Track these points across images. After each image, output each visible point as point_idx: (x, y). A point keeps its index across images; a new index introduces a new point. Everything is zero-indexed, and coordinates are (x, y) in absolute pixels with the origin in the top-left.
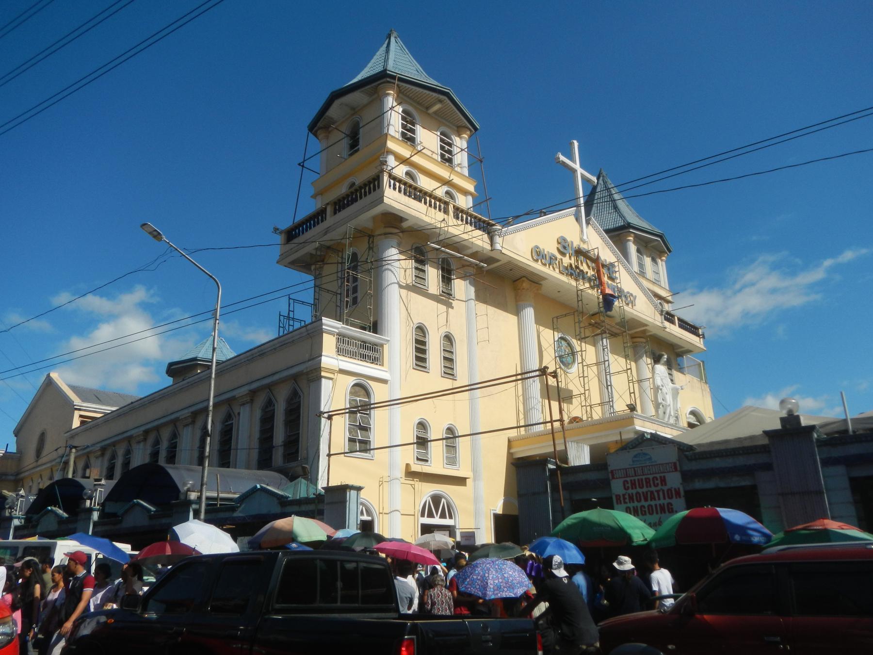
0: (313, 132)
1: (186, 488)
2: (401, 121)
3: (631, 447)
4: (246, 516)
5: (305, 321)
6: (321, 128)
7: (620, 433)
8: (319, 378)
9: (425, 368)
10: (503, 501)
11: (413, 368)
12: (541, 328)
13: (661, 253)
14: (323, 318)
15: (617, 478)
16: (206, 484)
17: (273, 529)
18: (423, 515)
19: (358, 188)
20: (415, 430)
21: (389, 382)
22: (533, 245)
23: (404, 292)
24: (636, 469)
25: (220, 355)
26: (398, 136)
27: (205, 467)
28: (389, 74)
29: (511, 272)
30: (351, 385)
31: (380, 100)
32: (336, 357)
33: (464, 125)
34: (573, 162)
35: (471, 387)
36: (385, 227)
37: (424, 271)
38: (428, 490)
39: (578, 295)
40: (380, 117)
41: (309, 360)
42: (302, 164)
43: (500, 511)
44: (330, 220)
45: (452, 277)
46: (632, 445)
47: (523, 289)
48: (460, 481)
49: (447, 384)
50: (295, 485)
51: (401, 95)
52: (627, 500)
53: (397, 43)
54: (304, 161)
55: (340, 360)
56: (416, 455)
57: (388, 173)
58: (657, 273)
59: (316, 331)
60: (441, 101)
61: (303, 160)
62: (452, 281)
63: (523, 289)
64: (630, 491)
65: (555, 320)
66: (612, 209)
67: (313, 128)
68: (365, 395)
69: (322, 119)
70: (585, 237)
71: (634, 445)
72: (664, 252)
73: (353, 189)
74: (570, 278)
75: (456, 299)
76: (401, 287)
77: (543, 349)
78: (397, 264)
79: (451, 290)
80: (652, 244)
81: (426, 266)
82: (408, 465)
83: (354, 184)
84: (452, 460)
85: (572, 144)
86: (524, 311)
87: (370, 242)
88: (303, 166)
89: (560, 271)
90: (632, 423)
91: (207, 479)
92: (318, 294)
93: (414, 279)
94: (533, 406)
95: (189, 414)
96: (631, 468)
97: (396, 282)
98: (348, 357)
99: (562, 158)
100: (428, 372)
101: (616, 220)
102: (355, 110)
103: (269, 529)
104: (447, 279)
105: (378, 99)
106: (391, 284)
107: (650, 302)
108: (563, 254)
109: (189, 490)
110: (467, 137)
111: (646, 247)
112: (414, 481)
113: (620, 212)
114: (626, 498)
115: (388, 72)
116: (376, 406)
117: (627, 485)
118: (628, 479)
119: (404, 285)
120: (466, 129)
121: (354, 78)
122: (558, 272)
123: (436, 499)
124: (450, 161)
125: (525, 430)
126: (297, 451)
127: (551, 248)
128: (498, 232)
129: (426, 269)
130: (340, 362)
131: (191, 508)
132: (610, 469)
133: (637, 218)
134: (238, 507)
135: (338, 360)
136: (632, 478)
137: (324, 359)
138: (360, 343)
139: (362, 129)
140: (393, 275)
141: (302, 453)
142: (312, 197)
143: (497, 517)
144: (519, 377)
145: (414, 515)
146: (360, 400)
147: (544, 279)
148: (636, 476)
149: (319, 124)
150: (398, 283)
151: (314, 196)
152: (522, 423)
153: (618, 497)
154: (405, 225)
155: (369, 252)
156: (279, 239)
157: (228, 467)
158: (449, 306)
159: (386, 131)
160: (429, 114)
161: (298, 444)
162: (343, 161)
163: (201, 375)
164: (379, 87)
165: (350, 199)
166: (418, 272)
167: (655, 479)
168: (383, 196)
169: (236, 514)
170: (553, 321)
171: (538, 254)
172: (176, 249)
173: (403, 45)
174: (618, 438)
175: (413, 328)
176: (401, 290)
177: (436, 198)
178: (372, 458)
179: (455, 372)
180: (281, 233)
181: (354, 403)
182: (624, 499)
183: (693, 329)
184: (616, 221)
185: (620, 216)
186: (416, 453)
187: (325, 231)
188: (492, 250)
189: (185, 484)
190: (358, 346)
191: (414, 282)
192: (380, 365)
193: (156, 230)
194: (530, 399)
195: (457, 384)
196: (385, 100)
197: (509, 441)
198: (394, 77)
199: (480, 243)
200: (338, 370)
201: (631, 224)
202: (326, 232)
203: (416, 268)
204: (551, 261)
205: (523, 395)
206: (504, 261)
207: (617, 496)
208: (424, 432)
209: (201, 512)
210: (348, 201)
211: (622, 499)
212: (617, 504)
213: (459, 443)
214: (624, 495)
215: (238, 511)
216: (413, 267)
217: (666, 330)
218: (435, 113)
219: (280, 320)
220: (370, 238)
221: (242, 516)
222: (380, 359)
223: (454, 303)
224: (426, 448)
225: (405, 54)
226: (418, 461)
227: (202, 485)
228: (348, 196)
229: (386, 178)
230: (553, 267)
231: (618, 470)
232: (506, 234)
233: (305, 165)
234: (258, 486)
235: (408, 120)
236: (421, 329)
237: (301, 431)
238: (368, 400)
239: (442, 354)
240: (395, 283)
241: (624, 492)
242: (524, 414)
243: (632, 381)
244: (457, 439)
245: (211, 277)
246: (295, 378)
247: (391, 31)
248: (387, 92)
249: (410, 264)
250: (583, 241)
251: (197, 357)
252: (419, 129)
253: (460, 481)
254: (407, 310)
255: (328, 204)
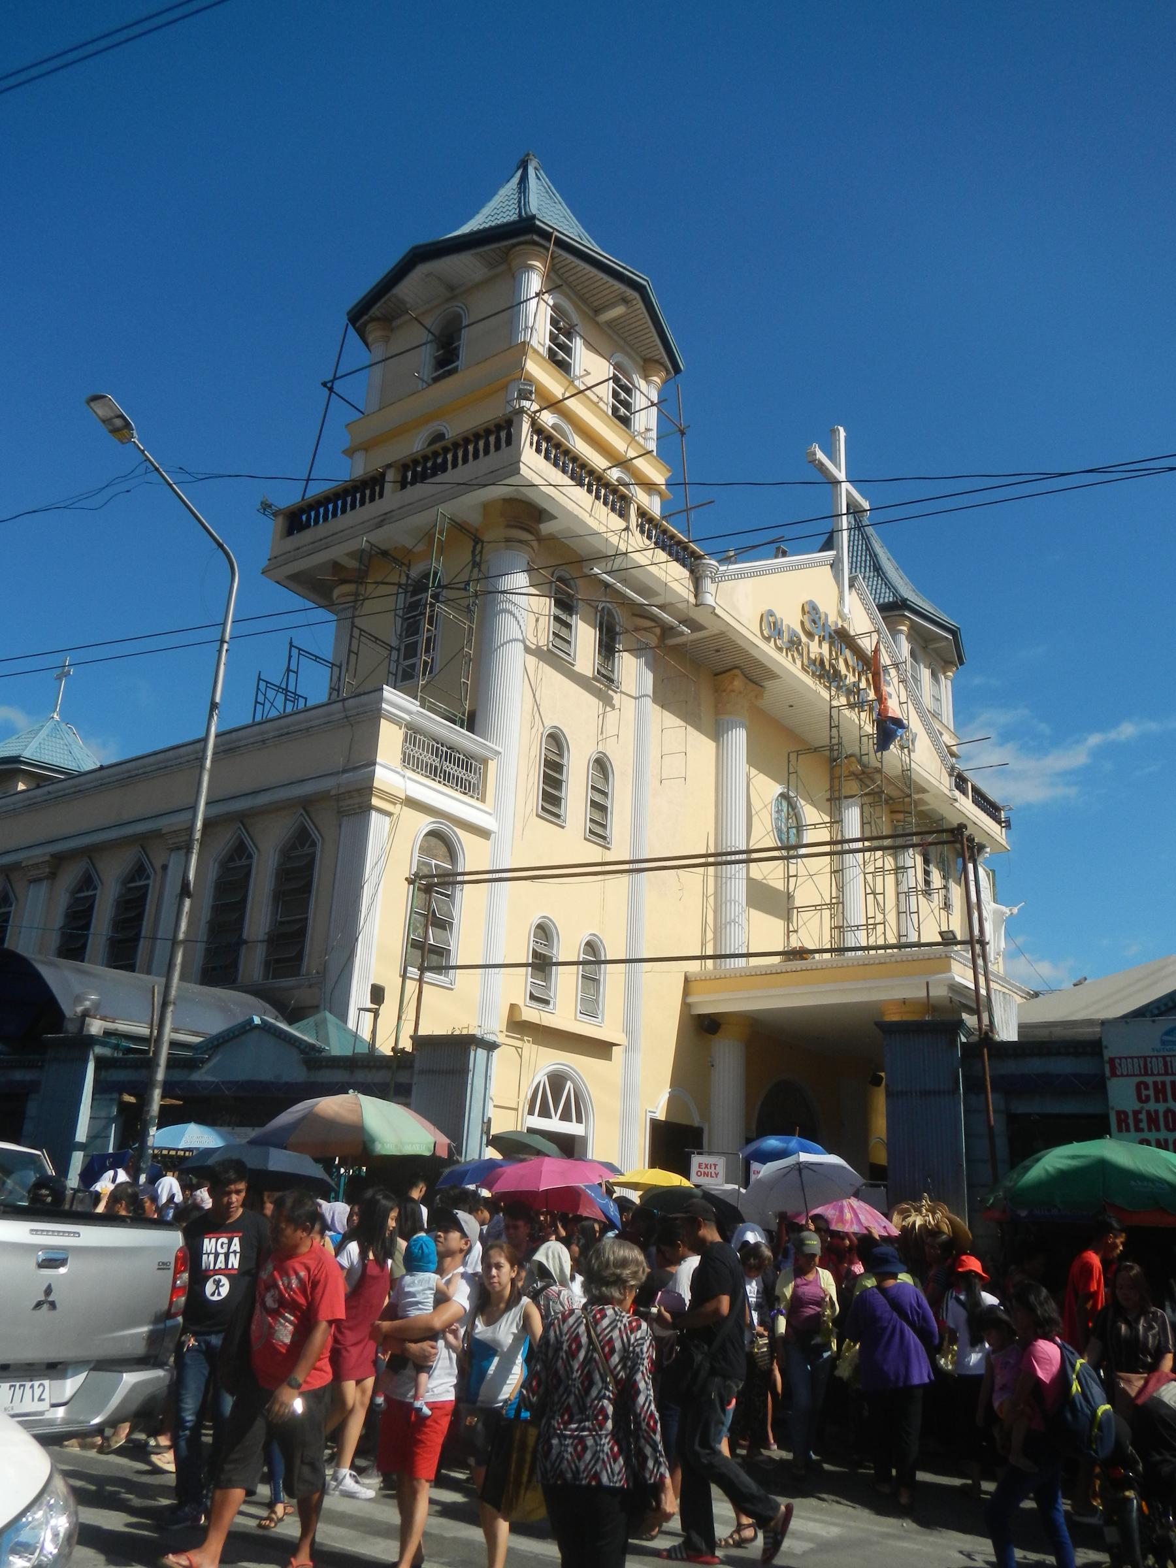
0: (358, 325)
1: (79, 1009)
2: (549, 327)
3: (1156, 1012)
4: (223, 1083)
5: (306, 699)
6: (376, 319)
7: (927, 984)
8: (366, 809)
9: (558, 816)
10: (668, 1095)
11: (538, 816)
12: (753, 772)
13: (947, 664)
14: (385, 686)
15: (1122, 1075)
16: (174, 1003)
17: (311, 1118)
18: (531, 1112)
19: (450, 446)
20: (532, 938)
21: (493, 835)
22: (765, 608)
23: (532, 660)
24: (1168, 1059)
25: (66, 757)
26: (543, 351)
27: (175, 965)
28: (538, 226)
29: (719, 654)
30: (424, 832)
31: (513, 276)
32: (402, 773)
33: (657, 357)
34: (836, 467)
35: (636, 867)
36: (509, 526)
37: (568, 626)
38: (549, 1060)
39: (831, 717)
40: (513, 306)
41: (344, 771)
42: (329, 385)
43: (661, 1116)
44: (392, 498)
45: (617, 646)
46: (1158, 1008)
47: (733, 691)
48: (601, 1049)
49: (593, 853)
50: (316, 1025)
51: (552, 275)
52: (1144, 1125)
53: (540, 179)
54: (335, 378)
55: (409, 779)
56: (529, 988)
57: (530, 416)
58: (938, 700)
59: (366, 712)
60: (625, 301)
61: (331, 378)
62: (617, 654)
63: (733, 691)
64: (1152, 1106)
65: (793, 757)
66: (870, 571)
67: (359, 316)
68: (445, 857)
69: (383, 300)
70: (846, 611)
71: (1163, 1008)
72: (952, 663)
73: (437, 446)
74: (818, 683)
75: (621, 692)
76: (527, 650)
77: (754, 812)
78: (521, 600)
79: (612, 671)
80: (937, 645)
81: (574, 616)
82: (513, 1007)
83: (440, 437)
84: (590, 1007)
85: (834, 432)
86: (730, 732)
87: (477, 552)
88: (331, 389)
89: (803, 665)
90: (949, 969)
91: (176, 991)
92: (357, 641)
93: (551, 639)
94: (733, 917)
95: (47, 858)
96: (1157, 1057)
97: (521, 638)
98: (422, 775)
99: (820, 455)
100: (563, 827)
101: (878, 591)
102: (453, 291)
103: (303, 1119)
104: (607, 649)
105: (513, 277)
106: (511, 641)
107: (935, 749)
108: (810, 635)
109: (86, 1014)
110: (659, 381)
111: (925, 648)
112: (523, 1040)
113: (887, 578)
114: (1141, 1121)
115: (538, 223)
116: (467, 878)
117: (1144, 1093)
118: (1149, 1080)
119: (533, 647)
120: (662, 368)
121: (464, 223)
122: (800, 668)
123: (557, 1081)
124: (625, 421)
125: (715, 964)
126: (299, 957)
127: (792, 620)
128: (711, 572)
129: (573, 624)
130: (410, 784)
131: (91, 1053)
132: (1107, 1054)
133: (914, 594)
134: (203, 1062)
135: (404, 777)
136: (1159, 1079)
137: (378, 769)
138: (445, 749)
139: (467, 329)
140: (516, 623)
141: (311, 963)
142: (344, 452)
143: (656, 1125)
144: (711, 860)
145: (516, 1110)
146: (436, 865)
147: (772, 676)
148: (1166, 1074)
149: (375, 311)
150: (523, 642)
151: (350, 452)
152: (710, 952)
153: (1122, 1116)
154: (546, 528)
155: (471, 572)
156: (271, 528)
157: (133, 971)
158: (608, 702)
159: (521, 339)
160: (597, 323)
161: (302, 943)
162: (420, 388)
163: (65, 783)
164: (514, 250)
165: (429, 464)
166: (558, 625)
167: (1142, 1086)
168: (519, 461)
169: (196, 1076)
170: (789, 757)
171: (772, 626)
172: (157, 469)
173: (550, 184)
174: (922, 994)
175: (542, 734)
176: (527, 655)
177: (607, 485)
178: (450, 986)
179: (608, 832)
180: (275, 514)
181: (425, 871)
182: (1137, 1121)
183: (990, 808)
184: (880, 594)
185: (886, 584)
186: (529, 984)
187: (382, 518)
188: (697, 605)
189: (79, 999)
190: (441, 756)
191: (550, 644)
192: (478, 799)
193: (122, 416)
194: (728, 904)
195: (610, 856)
196: (525, 277)
197: (687, 980)
198: (546, 236)
199: (675, 586)
200: (404, 798)
201: (908, 602)
202: (383, 521)
203: (557, 619)
204: (794, 645)
205: (715, 894)
206: (713, 628)
207: (1119, 1113)
208: (545, 945)
209: (158, 1065)
210: (425, 469)
211: (1131, 1121)
212: (1120, 1130)
213: (605, 973)
214: (1136, 1113)
215: (203, 1070)
216: (552, 614)
217: (957, 805)
218: (609, 323)
219: (258, 689)
220: (477, 543)
221: (213, 1082)
222: (478, 789)
223: (617, 698)
224: (547, 977)
225: (555, 203)
226: (533, 1002)
227: (165, 1004)
228: (426, 458)
229: (526, 426)
230: (793, 656)
231: (1126, 1058)
232: (725, 578)
233: (336, 389)
234: (257, 1020)
235: (562, 330)
236: (556, 740)
237: (311, 915)
238: (450, 867)
239: (590, 794)
240: (519, 640)
241: (1137, 1106)
242: (715, 933)
243: (915, 890)
244: (603, 965)
245: (220, 546)
246: (307, 804)
247: (528, 155)
248: (529, 262)
249: (545, 605)
250: (841, 614)
251: (20, 756)
252: (578, 345)
253: (601, 1049)
254: (534, 696)
255: (389, 466)
